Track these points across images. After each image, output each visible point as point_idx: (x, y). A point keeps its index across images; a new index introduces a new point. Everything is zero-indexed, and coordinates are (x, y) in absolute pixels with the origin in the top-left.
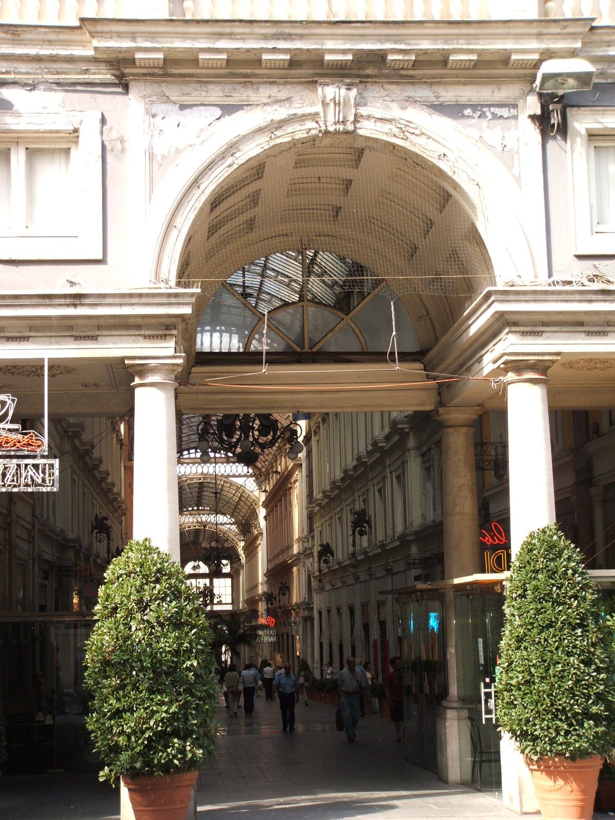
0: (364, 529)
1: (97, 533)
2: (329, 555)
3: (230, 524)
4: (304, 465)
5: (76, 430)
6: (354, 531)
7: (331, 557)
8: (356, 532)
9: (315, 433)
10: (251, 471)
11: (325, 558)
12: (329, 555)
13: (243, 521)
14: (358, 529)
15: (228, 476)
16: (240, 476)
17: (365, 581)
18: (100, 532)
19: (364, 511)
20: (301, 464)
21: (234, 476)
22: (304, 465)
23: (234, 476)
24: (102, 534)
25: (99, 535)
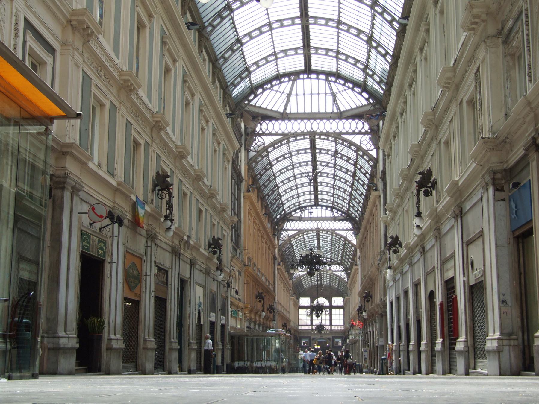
0: (428, 189)
1: (159, 190)
2: (398, 246)
3: (341, 271)
4: (382, 196)
5: (80, 18)
6: (418, 192)
7: (399, 248)
8: (422, 192)
9: (389, 156)
10: (351, 226)
11: (394, 248)
12: (398, 246)
13: (348, 266)
14: (423, 189)
15: (336, 230)
16: (343, 230)
17: (431, 249)
18: (162, 189)
19: (430, 172)
20: (380, 196)
21: (339, 230)
22: (382, 196)
23: (339, 230)
24: (163, 191)
25: (160, 192)
